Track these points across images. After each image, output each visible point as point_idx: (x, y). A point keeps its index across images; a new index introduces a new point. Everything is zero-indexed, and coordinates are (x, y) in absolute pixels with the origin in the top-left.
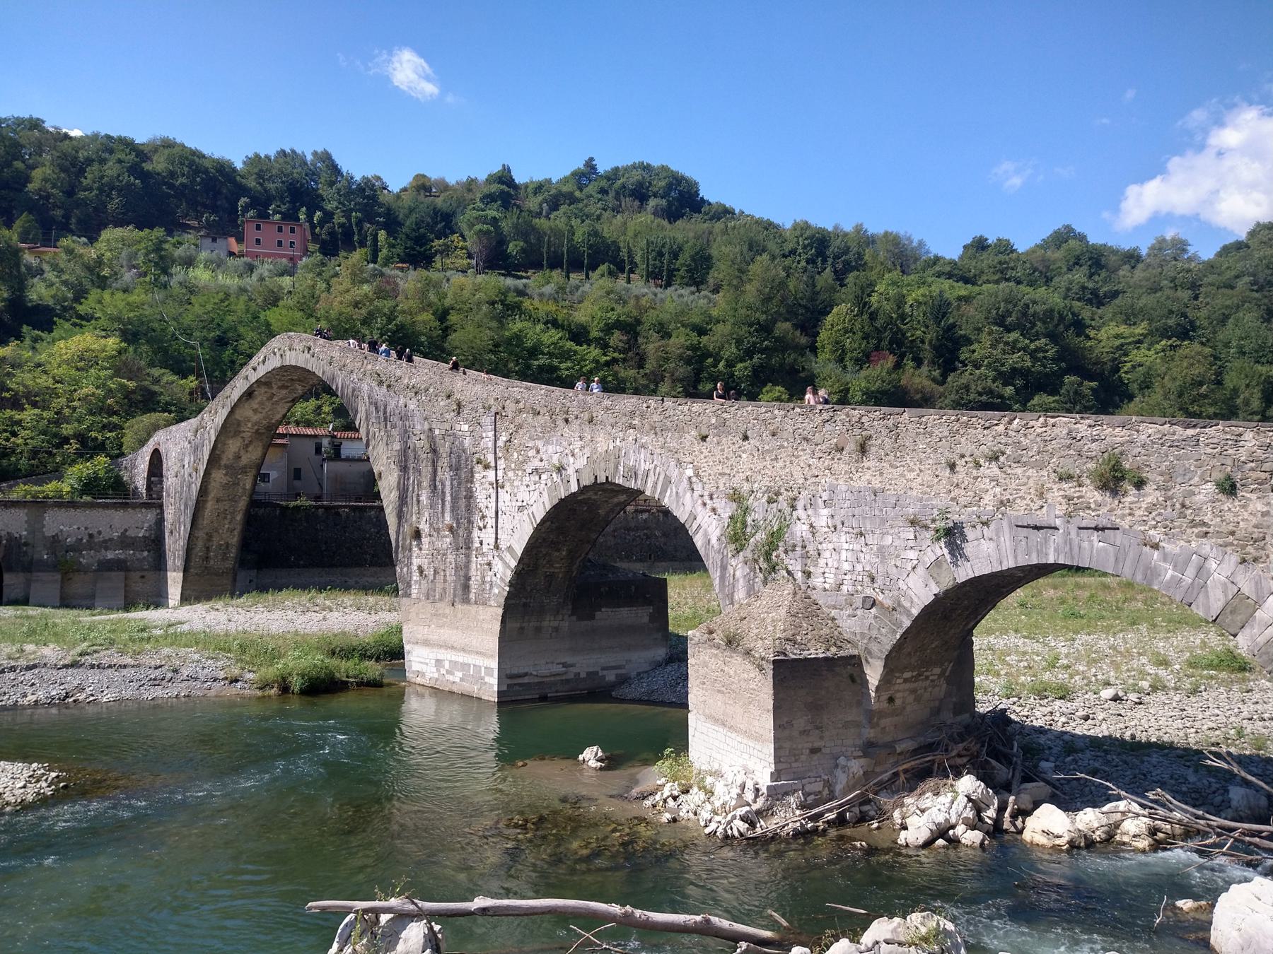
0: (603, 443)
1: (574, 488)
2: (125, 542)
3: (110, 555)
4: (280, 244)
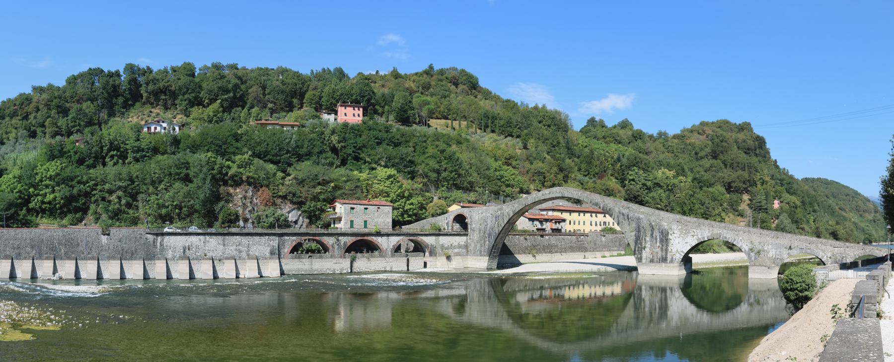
0: (716, 231)
1: (706, 239)
2: (460, 247)
3: (456, 250)
4: (354, 115)
